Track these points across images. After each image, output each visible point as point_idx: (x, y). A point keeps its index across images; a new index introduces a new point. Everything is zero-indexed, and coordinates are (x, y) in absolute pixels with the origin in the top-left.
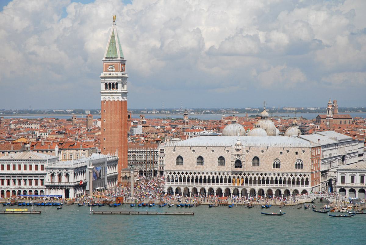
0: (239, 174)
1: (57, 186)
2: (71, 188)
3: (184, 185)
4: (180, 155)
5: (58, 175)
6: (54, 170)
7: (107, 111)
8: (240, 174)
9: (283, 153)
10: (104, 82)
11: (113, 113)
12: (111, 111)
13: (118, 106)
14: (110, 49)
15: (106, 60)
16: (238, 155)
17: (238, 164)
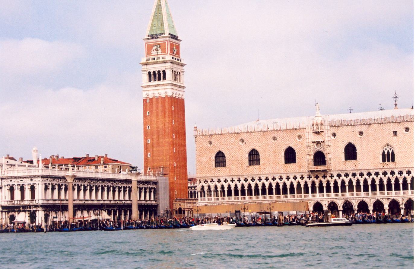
0: (322, 177)
1: (18, 207)
2: (39, 209)
3: (229, 201)
4: (220, 149)
5: (19, 188)
6: (13, 180)
7: (151, 112)
8: (324, 177)
9: (398, 133)
10: (146, 71)
11: (160, 114)
12: (158, 113)
13: (167, 104)
14: (154, 23)
15: (148, 39)
16: (318, 143)
17: (320, 158)
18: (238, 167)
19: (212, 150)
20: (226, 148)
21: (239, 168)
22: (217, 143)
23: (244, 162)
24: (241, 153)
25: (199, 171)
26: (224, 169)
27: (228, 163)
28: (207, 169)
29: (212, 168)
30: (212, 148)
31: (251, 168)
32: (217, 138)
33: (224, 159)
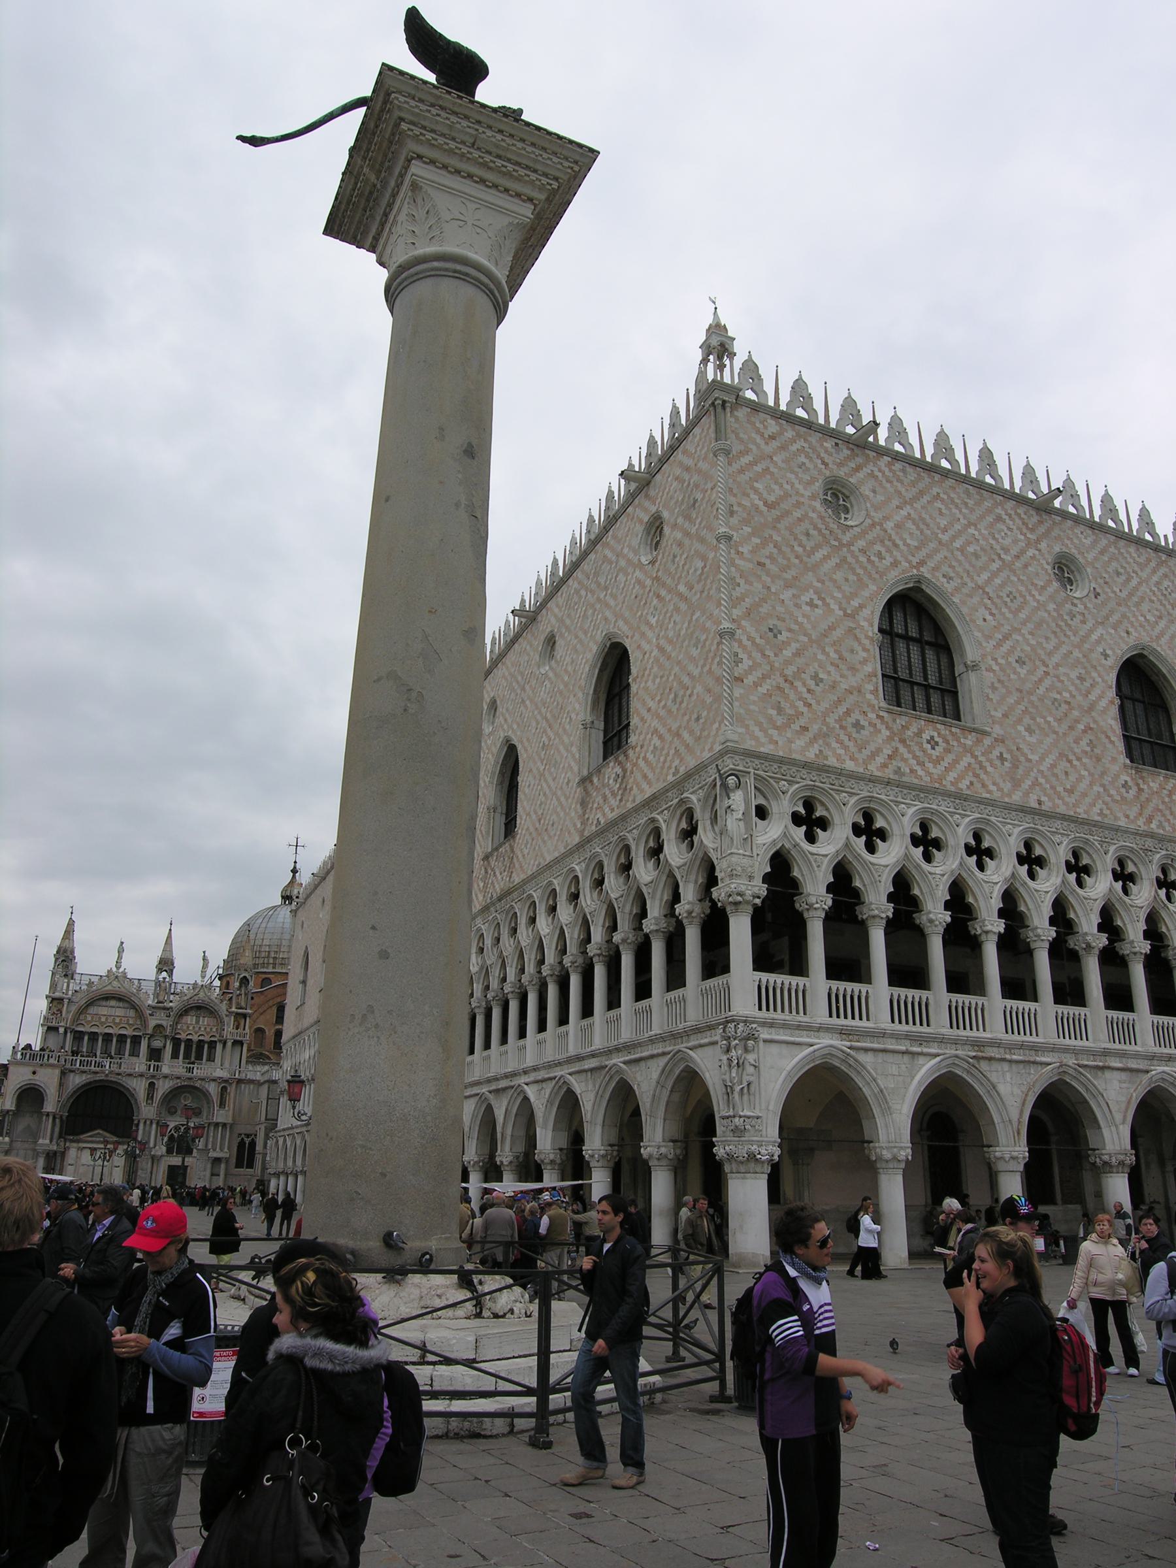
18: (1071, 757)
19: (863, 559)
20: (971, 585)
21: (1075, 762)
22: (897, 518)
23: (1102, 723)
24: (1077, 653)
25: (753, 698)
26: (969, 742)
27: (994, 697)
28: (825, 705)
29: (870, 705)
30: (861, 543)
31: (1155, 786)
32: (902, 482)
33: (932, 668)
